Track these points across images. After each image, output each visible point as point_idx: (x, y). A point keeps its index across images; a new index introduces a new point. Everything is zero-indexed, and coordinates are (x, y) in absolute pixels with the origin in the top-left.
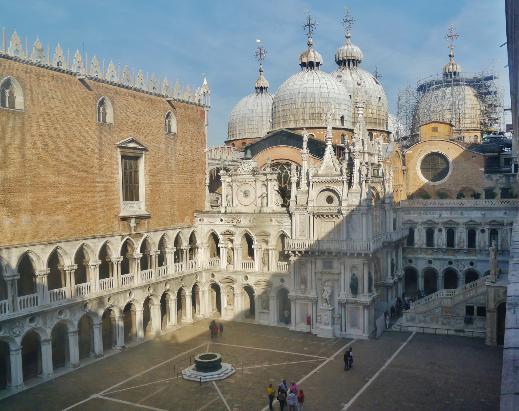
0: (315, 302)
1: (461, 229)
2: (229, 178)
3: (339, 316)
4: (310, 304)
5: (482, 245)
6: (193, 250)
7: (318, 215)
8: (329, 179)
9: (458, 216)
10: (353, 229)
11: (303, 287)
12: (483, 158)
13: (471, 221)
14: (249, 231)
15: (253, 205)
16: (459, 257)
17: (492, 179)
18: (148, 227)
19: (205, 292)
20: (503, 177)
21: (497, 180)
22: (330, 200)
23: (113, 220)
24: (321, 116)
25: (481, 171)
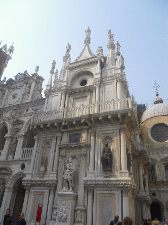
0: (53, 187)
3: (83, 208)
4: (47, 191)
11: (42, 169)
14: (7, 122)
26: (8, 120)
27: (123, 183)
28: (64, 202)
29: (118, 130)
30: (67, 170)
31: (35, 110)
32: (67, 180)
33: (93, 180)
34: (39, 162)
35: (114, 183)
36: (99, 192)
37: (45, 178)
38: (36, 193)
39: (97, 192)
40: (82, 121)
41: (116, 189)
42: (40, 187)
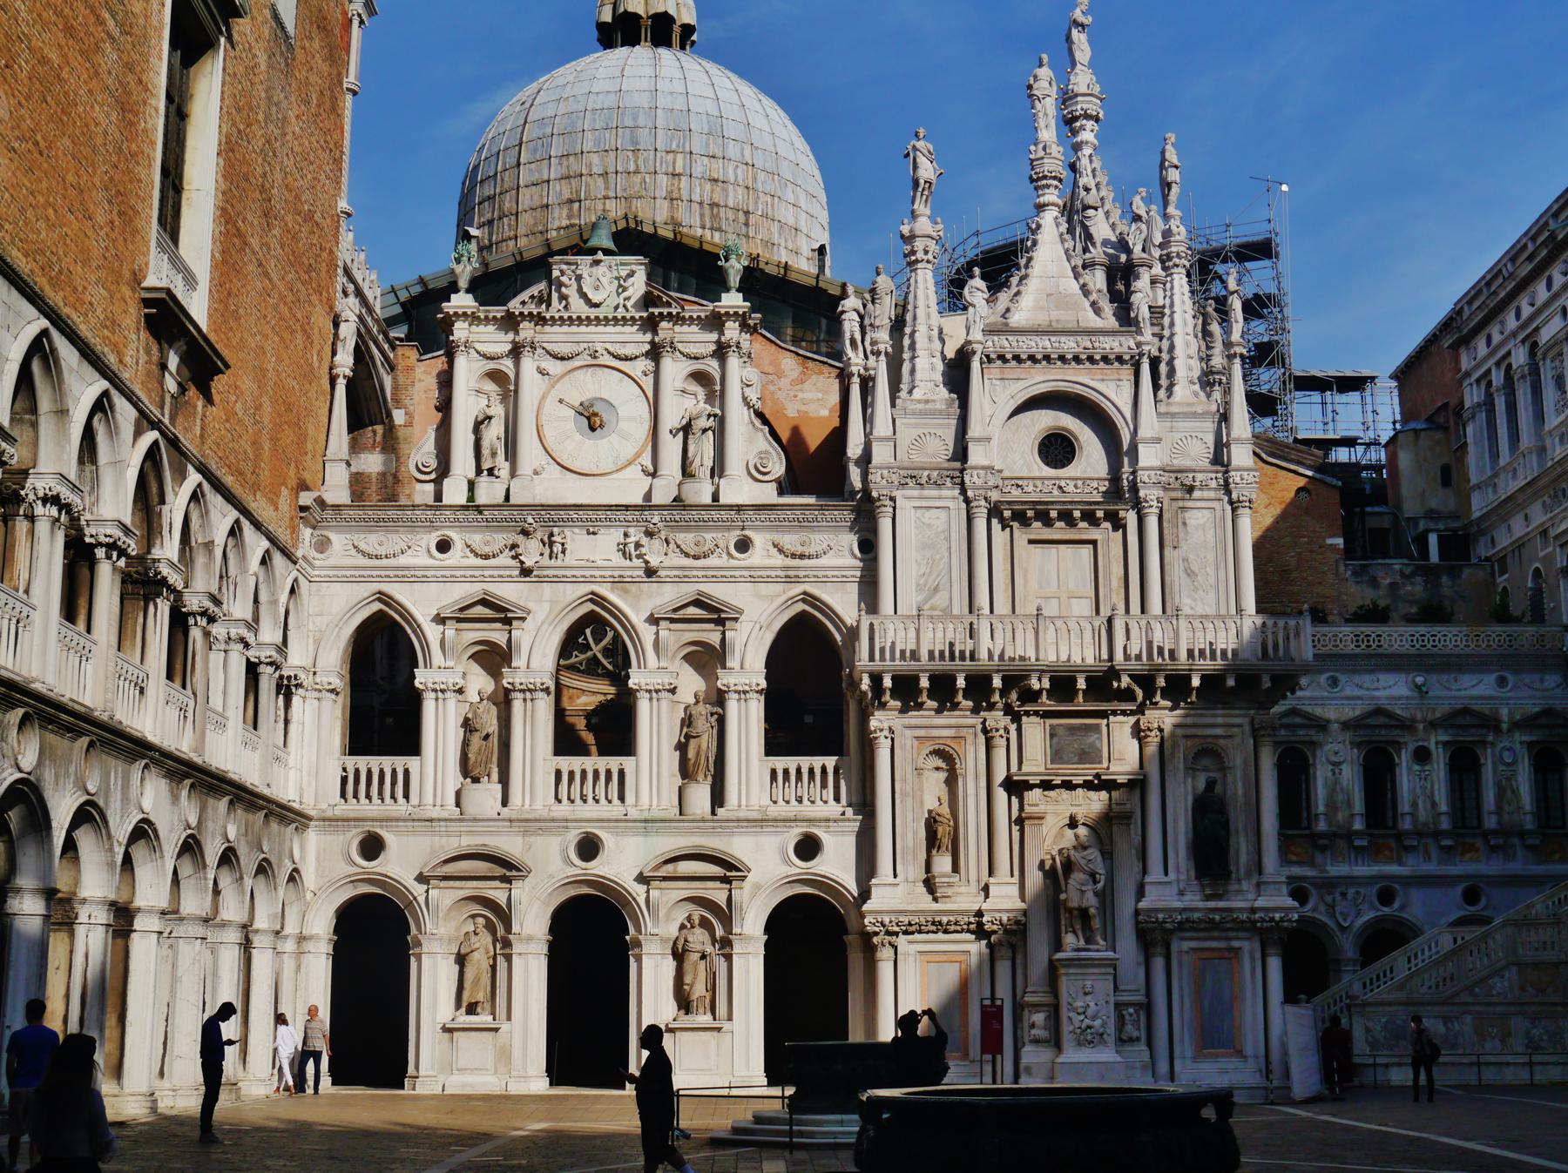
1: (1336, 747)
2: (501, 336)
5: (1422, 815)
6: (286, 689)
7: (1016, 515)
8: (1069, 345)
9: (1316, 694)
10: (1190, 573)
11: (943, 863)
12: (1336, 496)
13: (1379, 711)
15: (634, 472)
16: (1337, 869)
17: (1374, 583)
18: (202, 436)
19: (308, 946)
20: (1413, 574)
21: (1392, 585)
22: (1057, 449)
23: (126, 291)
24: (747, 224)
25: (1333, 547)
26: (618, 582)
27: (1277, 916)
28: (1088, 983)
29: (1247, 728)
30: (1077, 877)
31: (802, 556)
32: (1084, 913)
33: (1175, 910)
34: (915, 834)
35: (1244, 916)
36: (1186, 945)
37: (958, 899)
38: (929, 958)
39: (1181, 945)
40: (1124, 685)
41: (1241, 935)
42: (941, 936)
